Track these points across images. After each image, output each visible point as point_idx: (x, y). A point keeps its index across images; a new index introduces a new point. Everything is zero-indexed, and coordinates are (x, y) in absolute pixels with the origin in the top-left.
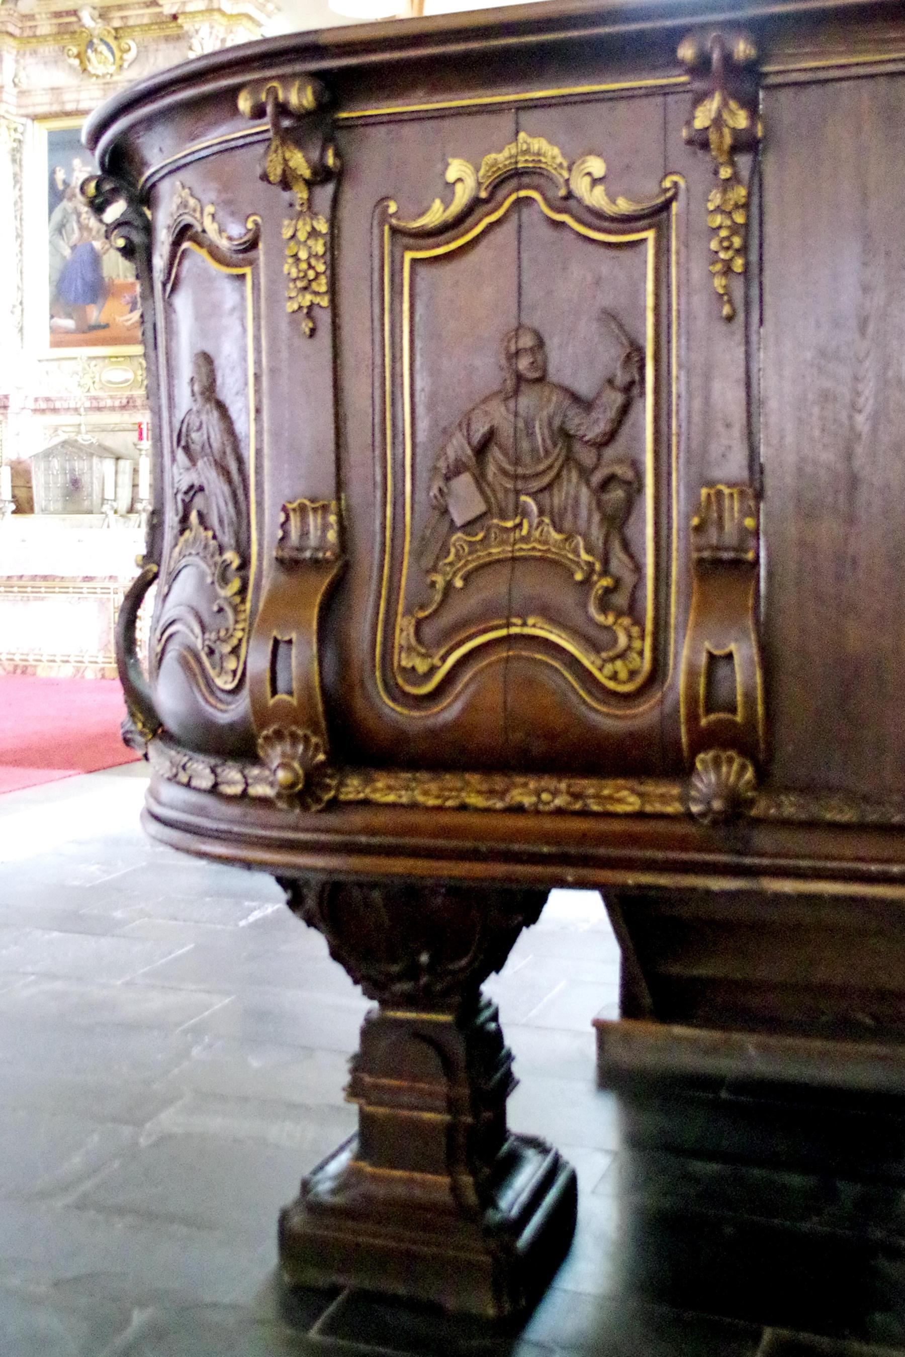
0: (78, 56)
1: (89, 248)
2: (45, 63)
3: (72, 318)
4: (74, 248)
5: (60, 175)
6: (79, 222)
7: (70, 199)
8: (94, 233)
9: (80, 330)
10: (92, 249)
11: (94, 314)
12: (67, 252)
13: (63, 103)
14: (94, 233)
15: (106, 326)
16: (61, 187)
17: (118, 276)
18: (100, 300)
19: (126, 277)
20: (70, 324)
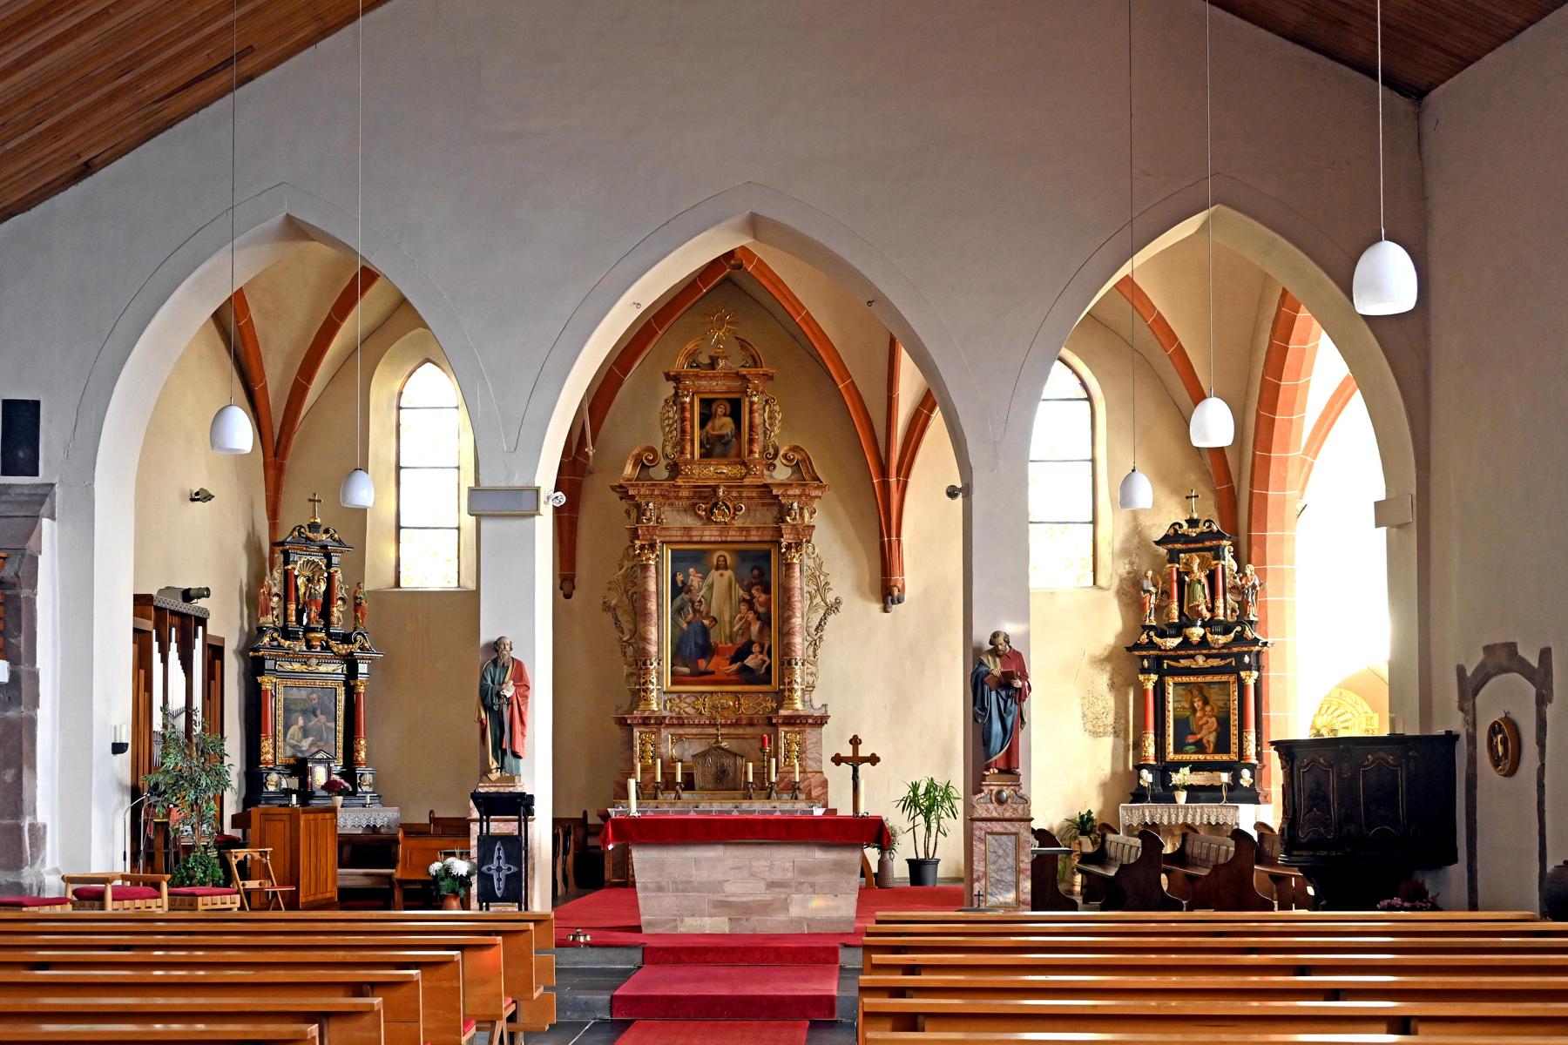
0: (705, 510)
1: (699, 624)
2: (678, 511)
3: (687, 666)
4: (689, 623)
5: (680, 578)
6: (693, 607)
7: (687, 593)
8: (704, 614)
9: (691, 675)
10: (703, 623)
11: (702, 664)
12: (685, 626)
13: (692, 536)
14: (704, 614)
15: (713, 673)
16: (680, 585)
17: (721, 642)
18: (708, 658)
19: (726, 643)
20: (686, 670)
